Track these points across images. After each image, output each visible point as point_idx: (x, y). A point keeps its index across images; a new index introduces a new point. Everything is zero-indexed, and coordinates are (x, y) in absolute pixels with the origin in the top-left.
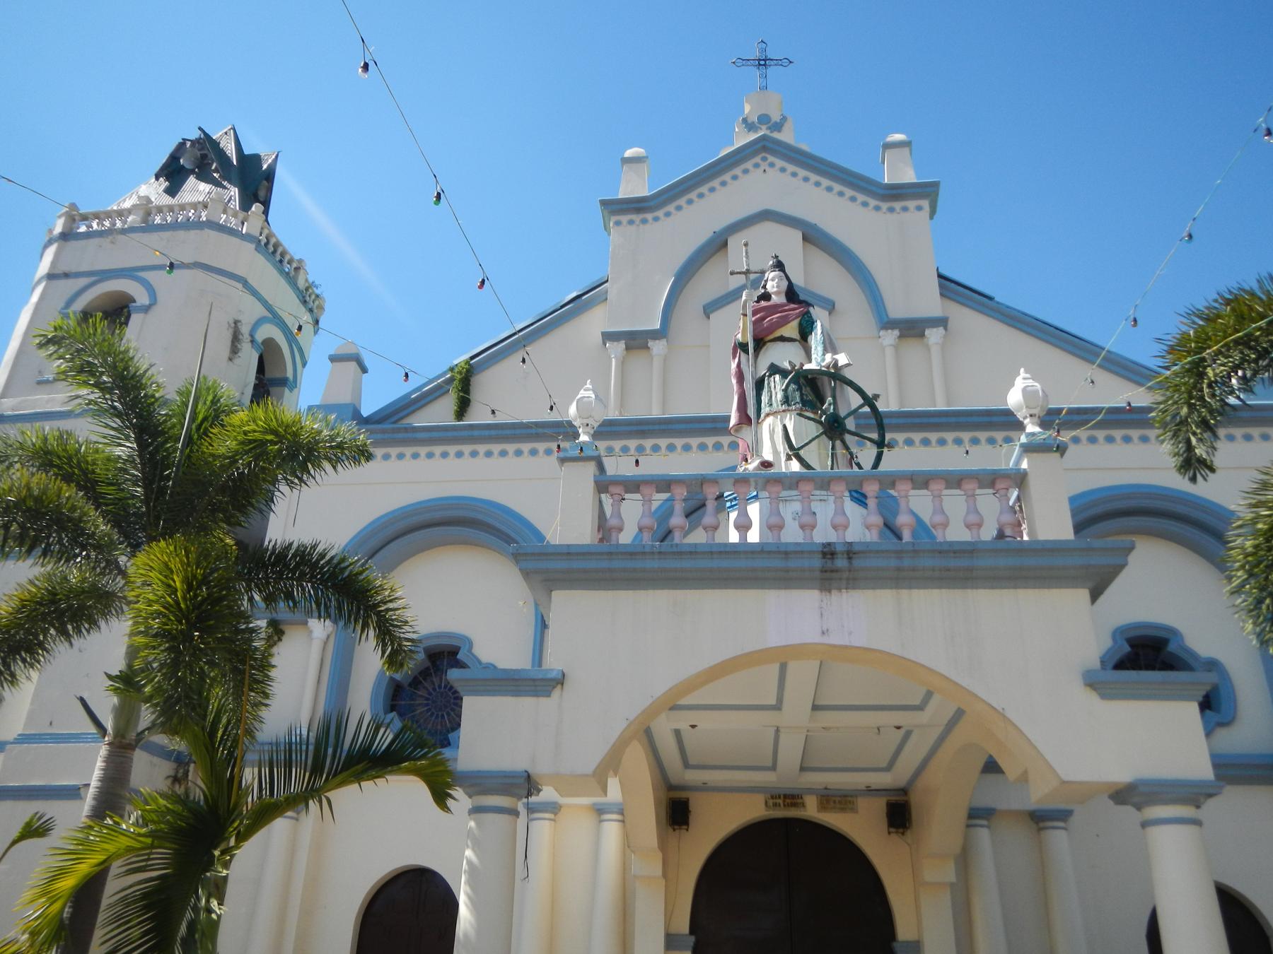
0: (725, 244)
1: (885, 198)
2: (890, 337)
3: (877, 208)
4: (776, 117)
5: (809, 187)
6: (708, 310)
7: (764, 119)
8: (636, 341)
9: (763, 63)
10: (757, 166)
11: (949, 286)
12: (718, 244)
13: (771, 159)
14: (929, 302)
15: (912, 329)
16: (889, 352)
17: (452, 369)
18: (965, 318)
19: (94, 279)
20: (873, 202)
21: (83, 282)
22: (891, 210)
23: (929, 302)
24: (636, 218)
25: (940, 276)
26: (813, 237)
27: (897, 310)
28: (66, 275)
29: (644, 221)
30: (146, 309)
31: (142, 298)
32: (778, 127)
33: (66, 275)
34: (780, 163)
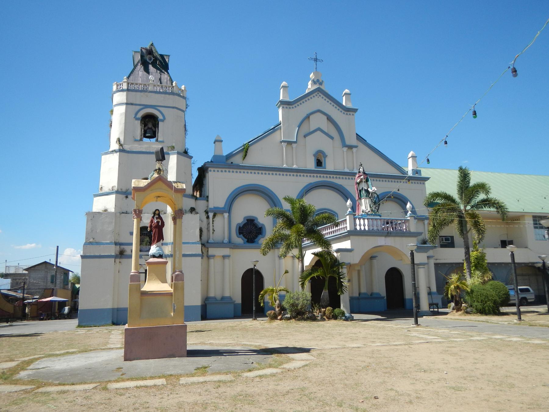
0: (309, 117)
1: (345, 111)
2: (345, 149)
3: (344, 113)
4: (321, 81)
5: (328, 104)
6: (305, 136)
7: (318, 80)
8: (290, 143)
9: (316, 60)
10: (316, 95)
11: (359, 137)
12: (308, 117)
13: (320, 94)
14: (353, 141)
15: (350, 147)
16: (345, 153)
17: (244, 146)
18: (361, 145)
19: (142, 107)
20: (343, 111)
21: (138, 108)
22: (347, 114)
23: (353, 141)
24: (288, 106)
25: (357, 134)
26: (329, 119)
27: (348, 143)
28: (132, 104)
29: (290, 108)
30: (163, 121)
31: (160, 117)
32: (321, 84)
33: (132, 104)
34: (322, 96)
